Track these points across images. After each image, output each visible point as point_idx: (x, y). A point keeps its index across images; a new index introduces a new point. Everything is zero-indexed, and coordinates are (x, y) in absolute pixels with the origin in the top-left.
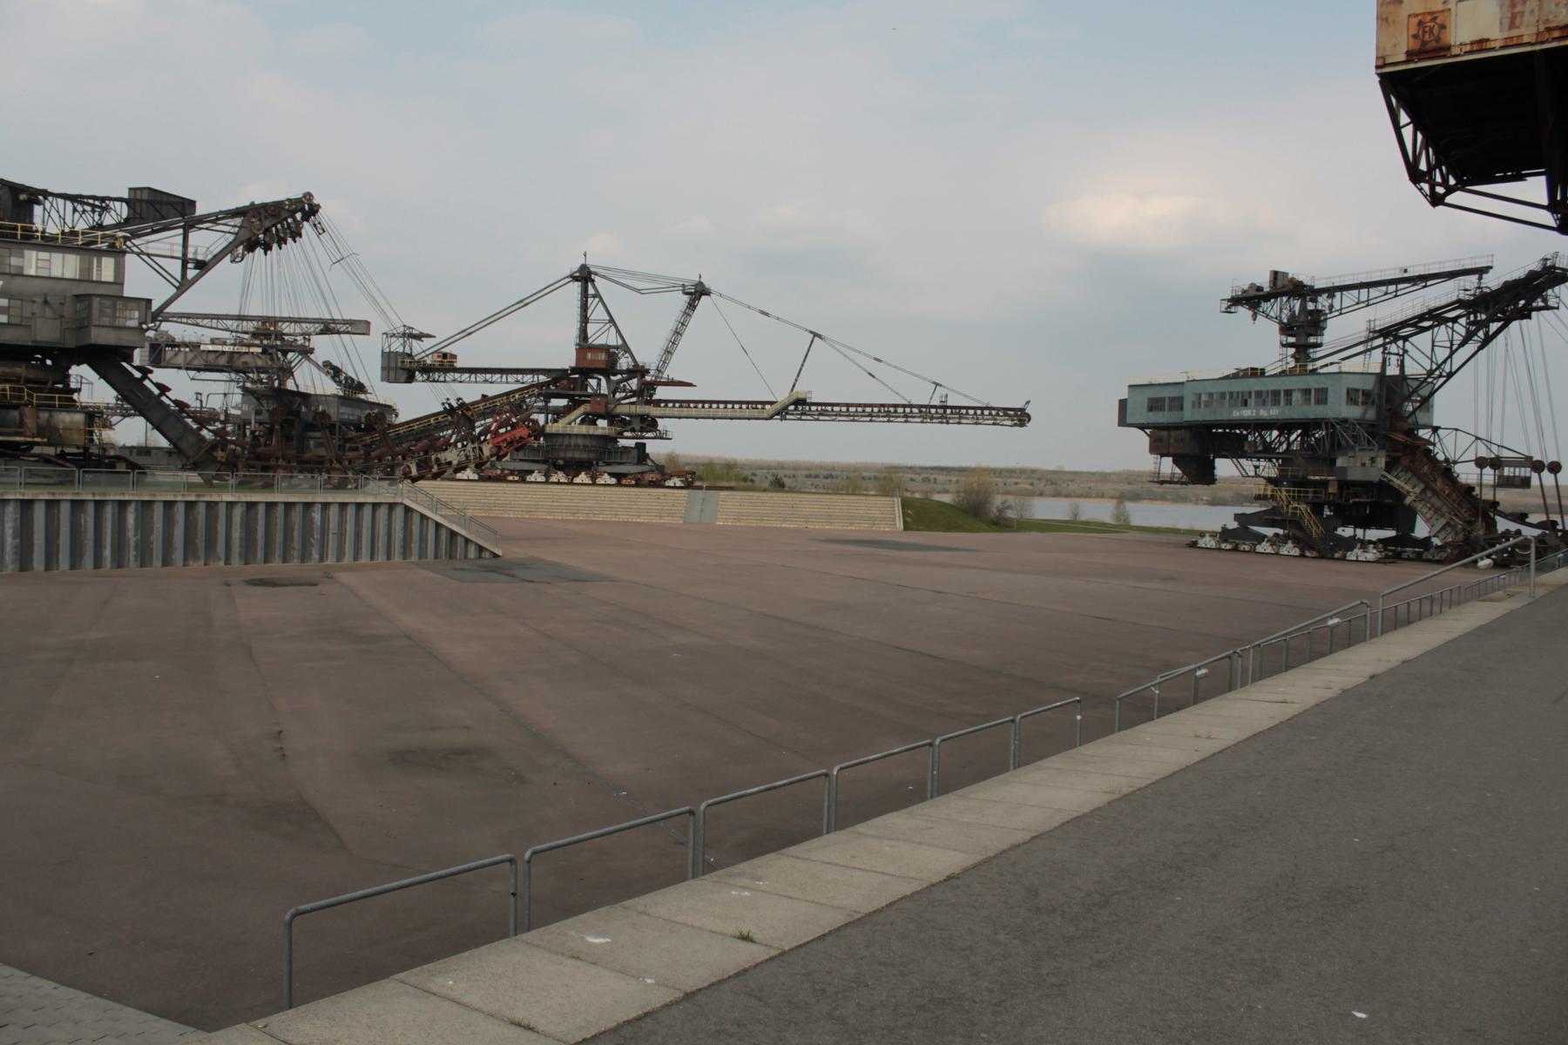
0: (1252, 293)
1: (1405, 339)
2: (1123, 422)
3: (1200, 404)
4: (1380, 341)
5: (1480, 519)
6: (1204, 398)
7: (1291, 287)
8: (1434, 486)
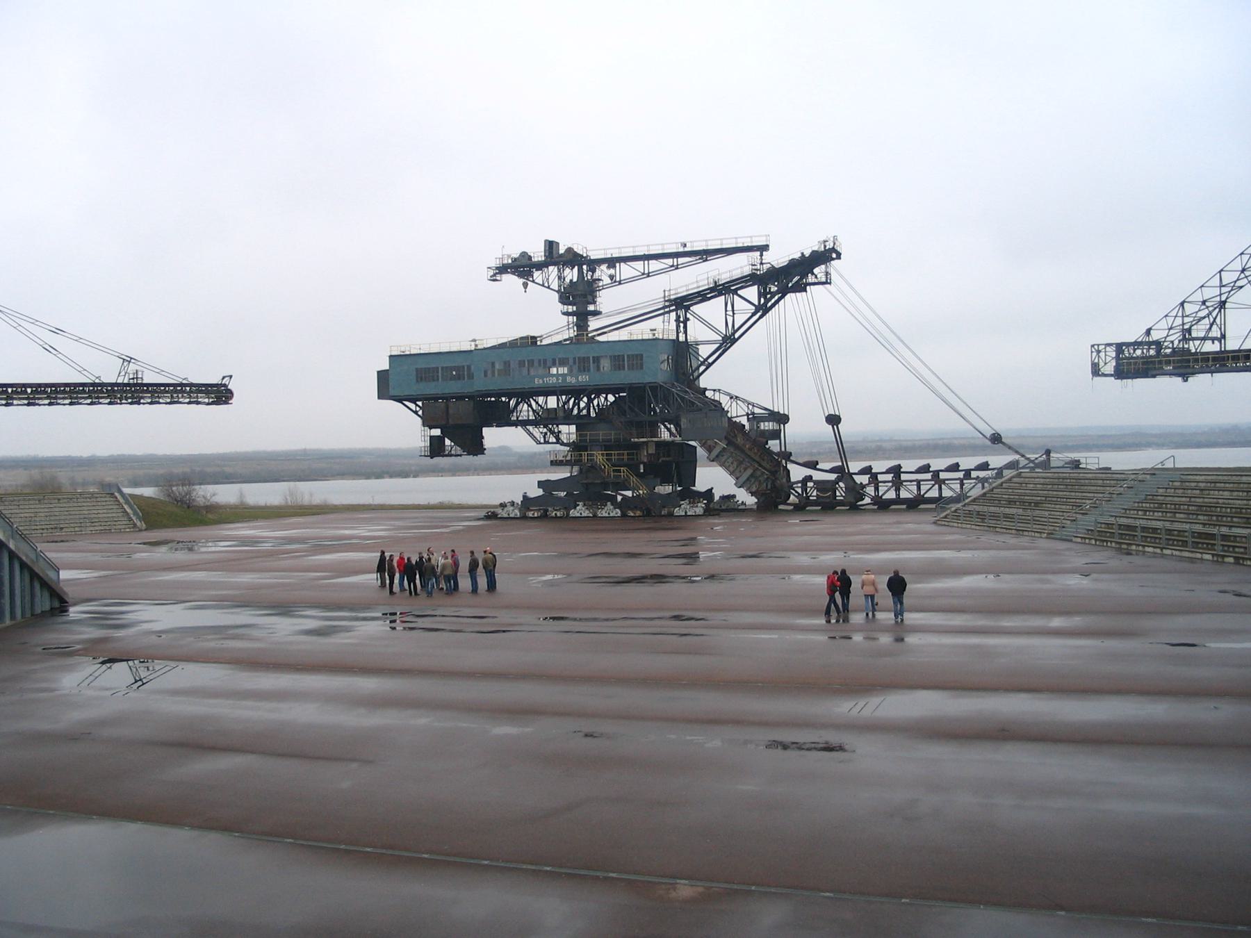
0: (525, 261)
1: (687, 308)
2: (383, 393)
3: (493, 372)
4: (674, 307)
5: (782, 469)
6: (497, 366)
7: (570, 256)
8: (735, 441)
